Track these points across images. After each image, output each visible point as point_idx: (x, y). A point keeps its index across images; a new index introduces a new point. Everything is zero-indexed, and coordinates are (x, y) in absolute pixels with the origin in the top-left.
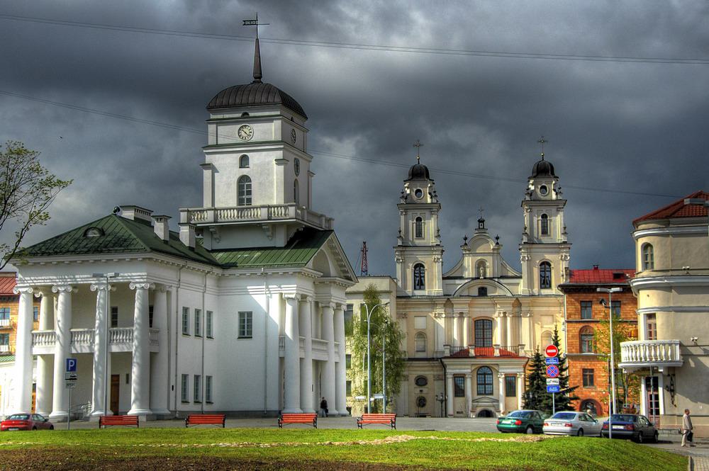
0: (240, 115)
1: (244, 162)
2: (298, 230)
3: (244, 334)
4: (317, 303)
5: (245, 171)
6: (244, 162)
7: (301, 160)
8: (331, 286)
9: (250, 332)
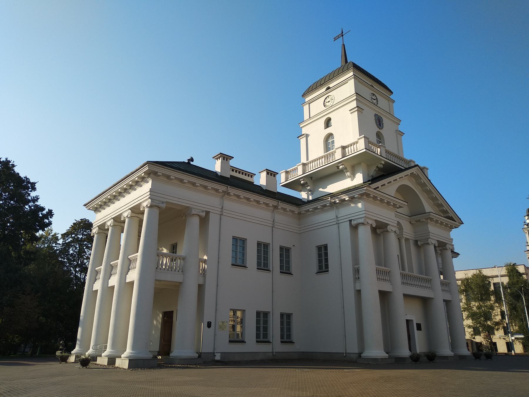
1: (328, 123)
4: (416, 242)
6: (328, 123)
8: (427, 223)
9: (327, 266)
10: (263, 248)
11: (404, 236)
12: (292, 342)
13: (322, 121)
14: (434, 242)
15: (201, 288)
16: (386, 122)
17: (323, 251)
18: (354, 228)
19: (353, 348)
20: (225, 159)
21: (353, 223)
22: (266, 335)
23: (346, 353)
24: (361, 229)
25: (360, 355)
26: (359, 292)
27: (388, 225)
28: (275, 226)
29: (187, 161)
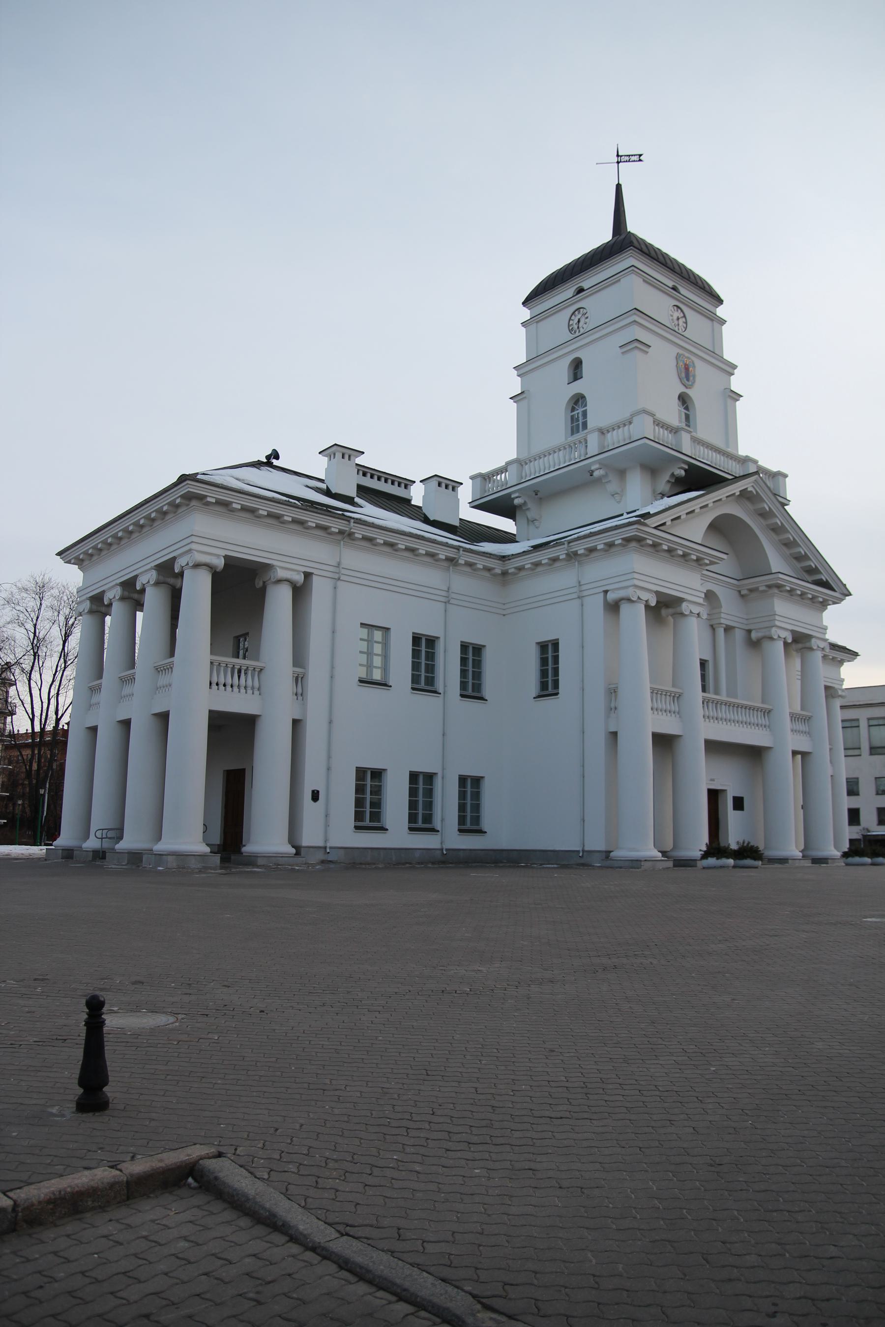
0: (570, 292)
2: (673, 475)
3: (547, 689)
5: (578, 387)
7: (697, 362)
10: (424, 647)
11: (722, 621)
12: (481, 832)
13: (563, 367)
14: (783, 634)
15: (296, 724)
16: (701, 370)
17: (549, 653)
18: (613, 608)
19: (596, 842)
20: (347, 457)
21: (611, 596)
22: (428, 818)
23: (583, 851)
24: (624, 608)
25: (608, 853)
26: (615, 734)
27: (680, 600)
28: (452, 601)
29: (265, 460)
